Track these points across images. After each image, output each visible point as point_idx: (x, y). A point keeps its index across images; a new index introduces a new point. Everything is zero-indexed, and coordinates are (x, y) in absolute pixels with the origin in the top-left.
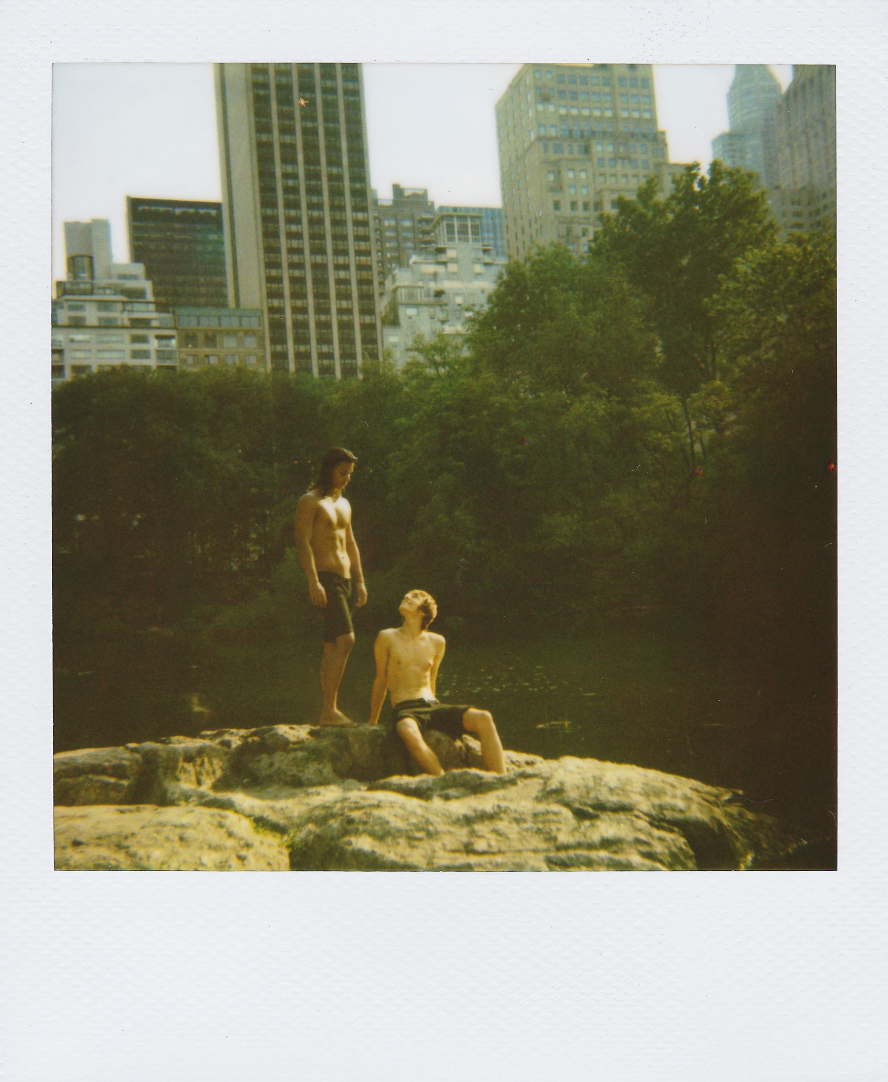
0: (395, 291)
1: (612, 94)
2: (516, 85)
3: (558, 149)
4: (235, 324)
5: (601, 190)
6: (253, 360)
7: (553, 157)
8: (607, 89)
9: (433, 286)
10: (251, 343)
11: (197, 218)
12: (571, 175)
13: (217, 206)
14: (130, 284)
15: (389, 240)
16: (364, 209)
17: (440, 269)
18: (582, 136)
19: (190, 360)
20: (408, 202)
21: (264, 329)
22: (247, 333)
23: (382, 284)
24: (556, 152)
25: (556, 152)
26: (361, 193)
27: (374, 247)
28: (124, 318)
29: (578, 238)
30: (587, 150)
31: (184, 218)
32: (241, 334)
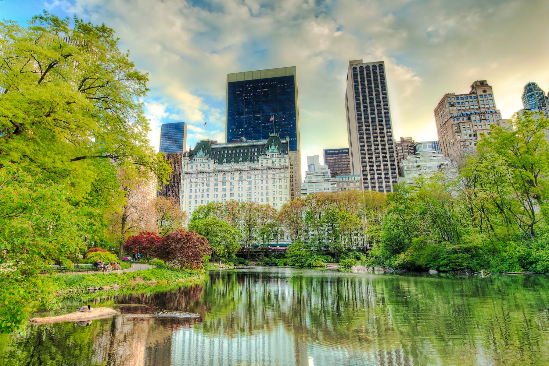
1: (478, 101)
4: (353, 179)
6: (358, 189)
8: (476, 100)
11: (345, 152)
13: (348, 149)
14: (324, 171)
15: (400, 153)
16: (392, 144)
18: (467, 115)
19: (340, 190)
22: (356, 181)
27: (395, 155)
28: (322, 180)
30: (469, 119)
31: (339, 153)
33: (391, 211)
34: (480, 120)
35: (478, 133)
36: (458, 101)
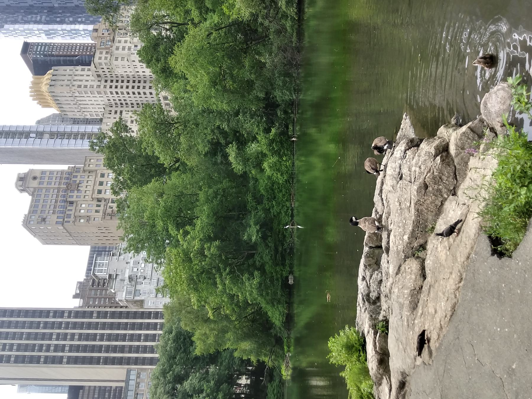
0: (127, 301)
2: (34, 233)
3: (69, 216)
5: (92, 198)
7: (72, 219)
9: (127, 281)
10: (143, 375)
12: (82, 211)
17: (119, 277)
20: (83, 291)
21: (138, 368)
23: (121, 307)
24: (70, 218)
25: (70, 218)
26: (77, 314)
29: (112, 211)
30: (71, 203)
32: (138, 380)
33: (435, 314)
34: (78, 190)
35: (96, 195)
36: (39, 212)
